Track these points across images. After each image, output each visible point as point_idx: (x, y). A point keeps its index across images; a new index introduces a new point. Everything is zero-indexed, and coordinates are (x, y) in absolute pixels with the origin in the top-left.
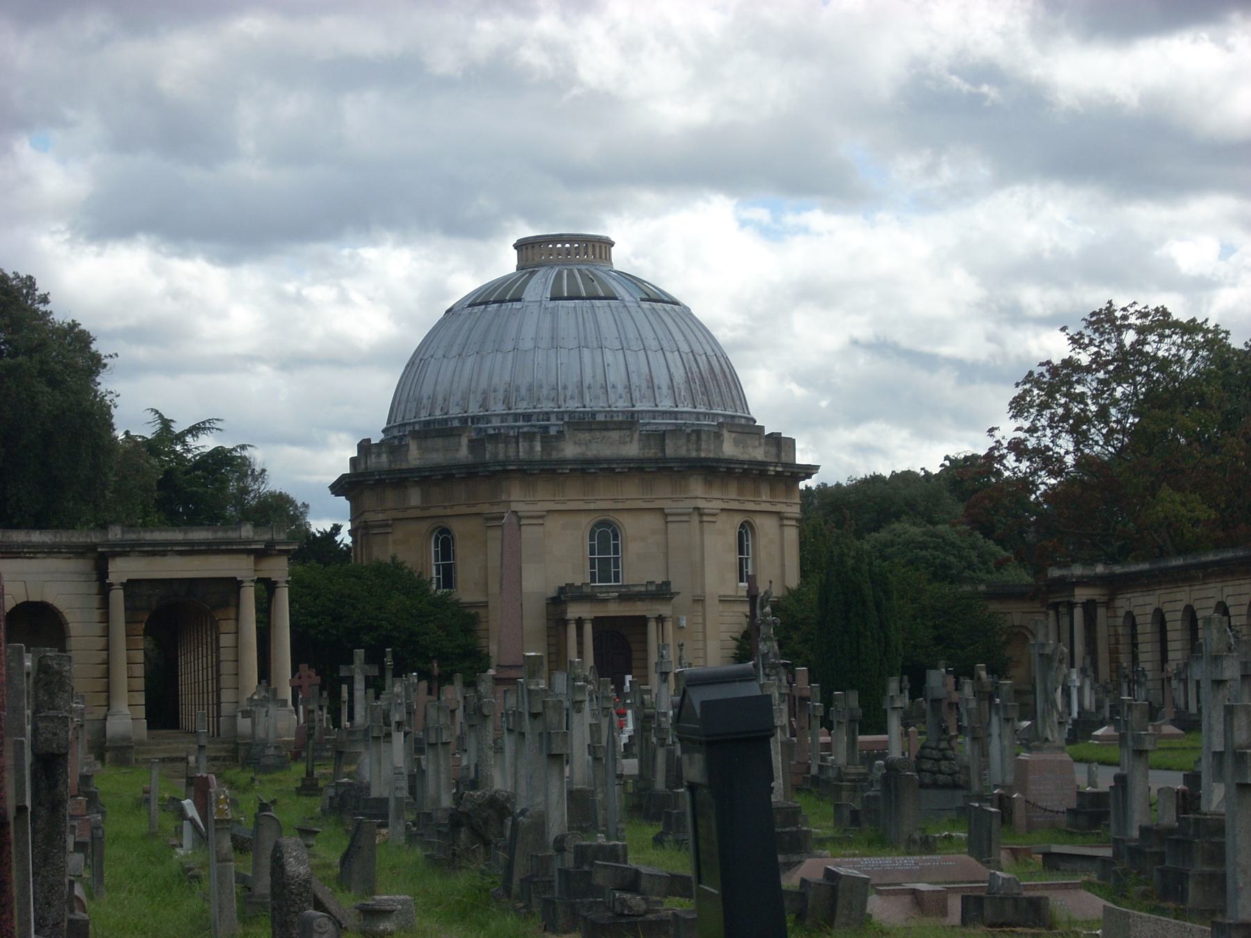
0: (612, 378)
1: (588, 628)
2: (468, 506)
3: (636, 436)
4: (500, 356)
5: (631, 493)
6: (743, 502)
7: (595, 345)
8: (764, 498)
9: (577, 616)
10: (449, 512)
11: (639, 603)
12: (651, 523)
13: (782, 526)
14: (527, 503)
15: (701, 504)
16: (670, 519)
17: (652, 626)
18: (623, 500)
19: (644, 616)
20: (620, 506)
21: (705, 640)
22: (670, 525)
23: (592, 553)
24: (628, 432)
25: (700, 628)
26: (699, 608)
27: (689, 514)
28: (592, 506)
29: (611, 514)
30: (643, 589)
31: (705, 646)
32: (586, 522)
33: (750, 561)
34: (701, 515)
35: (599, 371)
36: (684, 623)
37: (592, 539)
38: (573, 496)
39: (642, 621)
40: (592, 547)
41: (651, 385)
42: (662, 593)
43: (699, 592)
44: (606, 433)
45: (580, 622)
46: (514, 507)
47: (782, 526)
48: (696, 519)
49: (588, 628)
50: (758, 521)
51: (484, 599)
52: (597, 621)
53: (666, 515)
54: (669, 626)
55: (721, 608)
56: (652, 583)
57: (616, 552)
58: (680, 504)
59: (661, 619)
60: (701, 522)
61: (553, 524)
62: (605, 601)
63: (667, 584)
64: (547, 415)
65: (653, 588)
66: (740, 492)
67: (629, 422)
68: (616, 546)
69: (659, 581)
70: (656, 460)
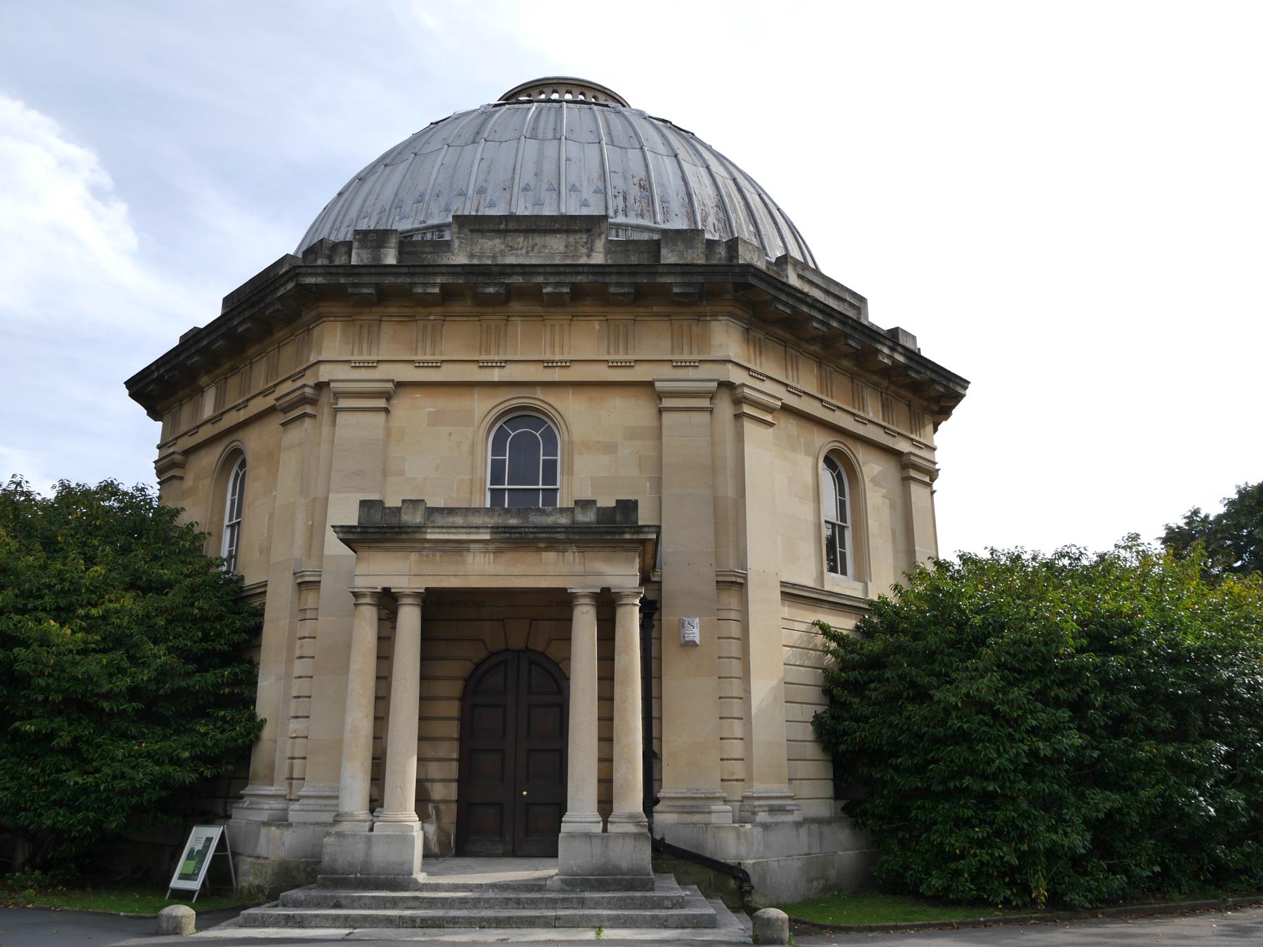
0: (571, 175)
2: (265, 393)
3: (600, 244)
4: (389, 168)
5: (583, 346)
7: (550, 136)
8: (871, 416)
9: (379, 584)
10: (242, 415)
11: (550, 556)
12: (628, 412)
13: (906, 480)
14: (357, 365)
15: (737, 376)
16: (667, 403)
17: (585, 623)
18: (566, 364)
19: (565, 589)
21: (746, 676)
22: (664, 414)
23: (497, 477)
24: (585, 237)
26: (731, 599)
27: (712, 396)
28: (496, 375)
29: (539, 393)
31: (747, 691)
32: (483, 407)
34: (738, 401)
35: (549, 167)
36: (694, 633)
37: (498, 448)
38: (456, 351)
41: (646, 186)
42: (616, 528)
43: (731, 564)
44: (539, 240)
45: (387, 602)
46: (325, 373)
47: (906, 480)
48: (725, 409)
49: (409, 619)
52: (439, 607)
53: (660, 396)
54: (630, 621)
55: (787, 611)
57: (550, 475)
58: (691, 373)
60: (739, 416)
61: (409, 411)
62: (459, 547)
63: (628, 507)
64: (440, 228)
65: (588, 517)
66: (824, 384)
67: (589, 225)
68: (551, 468)
70: (632, 270)
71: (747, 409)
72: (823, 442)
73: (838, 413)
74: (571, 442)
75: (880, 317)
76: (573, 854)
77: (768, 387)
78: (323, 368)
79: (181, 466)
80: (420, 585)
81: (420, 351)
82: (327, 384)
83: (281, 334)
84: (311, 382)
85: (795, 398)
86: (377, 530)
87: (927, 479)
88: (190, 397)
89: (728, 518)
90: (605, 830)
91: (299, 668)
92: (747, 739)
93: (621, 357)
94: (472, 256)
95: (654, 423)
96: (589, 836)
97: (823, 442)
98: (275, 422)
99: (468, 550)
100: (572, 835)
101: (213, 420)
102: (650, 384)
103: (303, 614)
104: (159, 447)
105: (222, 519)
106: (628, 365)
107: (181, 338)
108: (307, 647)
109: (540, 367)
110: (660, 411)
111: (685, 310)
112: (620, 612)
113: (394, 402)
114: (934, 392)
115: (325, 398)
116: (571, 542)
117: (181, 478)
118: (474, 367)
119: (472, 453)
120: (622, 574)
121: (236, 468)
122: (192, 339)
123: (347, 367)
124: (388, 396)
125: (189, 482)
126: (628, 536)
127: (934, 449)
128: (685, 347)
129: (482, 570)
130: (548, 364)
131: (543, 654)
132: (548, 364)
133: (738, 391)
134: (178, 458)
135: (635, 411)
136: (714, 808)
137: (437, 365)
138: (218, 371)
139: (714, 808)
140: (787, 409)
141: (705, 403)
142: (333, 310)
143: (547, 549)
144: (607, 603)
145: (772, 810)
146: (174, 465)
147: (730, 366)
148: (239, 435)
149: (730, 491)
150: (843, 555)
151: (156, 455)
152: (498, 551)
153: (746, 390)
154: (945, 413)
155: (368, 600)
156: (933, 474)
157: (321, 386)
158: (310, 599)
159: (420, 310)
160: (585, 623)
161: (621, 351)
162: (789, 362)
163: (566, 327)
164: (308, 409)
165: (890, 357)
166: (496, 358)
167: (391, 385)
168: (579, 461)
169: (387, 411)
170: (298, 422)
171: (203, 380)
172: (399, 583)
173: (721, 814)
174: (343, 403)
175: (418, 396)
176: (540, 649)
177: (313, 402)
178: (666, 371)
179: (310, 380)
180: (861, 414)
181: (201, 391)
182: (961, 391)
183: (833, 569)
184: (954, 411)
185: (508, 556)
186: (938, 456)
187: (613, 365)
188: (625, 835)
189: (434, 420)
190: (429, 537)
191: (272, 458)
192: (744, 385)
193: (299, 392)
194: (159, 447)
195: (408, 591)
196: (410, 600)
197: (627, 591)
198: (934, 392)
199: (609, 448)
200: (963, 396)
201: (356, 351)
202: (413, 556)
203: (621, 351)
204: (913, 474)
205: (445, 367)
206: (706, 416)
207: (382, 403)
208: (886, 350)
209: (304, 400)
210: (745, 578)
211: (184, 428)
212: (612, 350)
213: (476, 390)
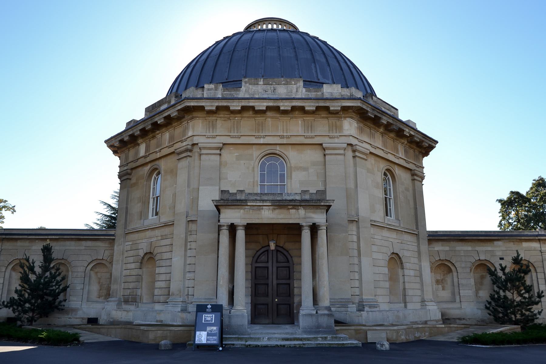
1: (241, 234)
2: (169, 147)
6: (387, 153)
8: (400, 156)
9: (230, 221)
10: (158, 155)
11: (293, 211)
12: (312, 156)
13: (414, 180)
15: (354, 142)
17: (306, 235)
19: (299, 224)
20: (285, 141)
23: (262, 181)
25: (355, 245)
26: (353, 227)
28: (262, 141)
29: (278, 148)
30: (298, 198)
31: (360, 261)
32: (256, 153)
33: (392, 201)
34: (354, 151)
37: (262, 170)
39: (296, 229)
40: (262, 176)
45: (232, 229)
46: (196, 140)
48: (350, 154)
49: (241, 234)
50: (397, 171)
51: (171, 219)
54: (322, 235)
56: (304, 192)
57: (282, 180)
58: (336, 140)
59: (314, 229)
60: (354, 157)
61: (228, 155)
65: (307, 197)
68: (282, 176)
69: (313, 190)
71: (357, 154)
72: (383, 166)
73: (389, 155)
74: (291, 167)
75: (403, 116)
76: (303, 321)
77: (365, 145)
78: (195, 138)
79: (130, 174)
80: (245, 222)
81: (232, 132)
82: (197, 144)
83: (176, 124)
84: (190, 143)
85: (374, 149)
86: (226, 201)
87: (420, 179)
88: (134, 147)
89: (351, 197)
90: (317, 313)
91: (189, 253)
92: (360, 280)
93: (310, 134)
94: (249, 94)
95: (322, 159)
96: (311, 315)
97: (383, 166)
98: (174, 158)
99: (262, 209)
100: (304, 315)
101: (145, 157)
102: (321, 144)
103: (188, 232)
104: (119, 167)
105: (149, 195)
106: (312, 137)
107: (128, 124)
108: (193, 245)
109: (279, 138)
110: (325, 155)
111: (334, 116)
112: (319, 232)
113: (222, 151)
114: (423, 145)
115: (196, 149)
116: (301, 206)
117: (130, 179)
118: (253, 138)
119: (253, 171)
120: (319, 218)
121: (154, 175)
122: (132, 125)
123: (204, 137)
124: (221, 149)
125: (134, 181)
126: (322, 204)
127: (423, 168)
128: (334, 130)
129: (268, 215)
130: (282, 137)
131: (282, 247)
132: (282, 137)
133: (354, 147)
134: (129, 171)
135: (315, 155)
136: (349, 306)
137: (239, 137)
138: (147, 138)
139: (349, 306)
140: (371, 153)
141: (342, 152)
142: (198, 115)
143: (291, 209)
144: (314, 229)
145: (370, 307)
146: (128, 174)
147: (351, 137)
148: (157, 162)
149: (352, 186)
150: (390, 209)
151: (118, 170)
152: (274, 209)
153: (357, 147)
154: (426, 154)
155: (225, 228)
156: (423, 178)
157: (193, 145)
158: (193, 226)
159: (232, 115)
160: (306, 235)
161: (310, 132)
162: (372, 136)
163: (288, 122)
164: (189, 154)
165: (409, 133)
166: (262, 134)
167: (222, 145)
168: (294, 174)
169: (220, 155)
170: (185, 159)
171: (140, 141)
172: (236, 221)
173: (353, 308)
174: (204, 151)
175: (232, 148)
176: (281, 246)
177: (191, 151)
178: (327, 139)
179: (189, 142)
180: (397, 155)
181: (139, 145)
182: (433, 145)
183: (387, 215)
184: (430, 153)
185: (277, 211)
186: (425, 171)
187: (306, 137)
188: (324, 315)
189: (238, 158)
190: (249, 204)
191: (173, 172)
192: (356, 145)
193: (185, 147)
194: (119, 167)
195: (240, 224)
196: (241, 228)
197: (322, 224)
198: (423, 145)
199: (305, 169)
200: (434, 147)
201: (208, 131)
202: (242, 211)
203: (310, 132)
204: (416, 177)
205: (242, 138)
206: (342, 157)
207: (218, 152)
208: (407, 130)
209: (187, 150)
210: (358, 219)
211: (131, 159)
212: (306, 131)
213: (254, 146)
